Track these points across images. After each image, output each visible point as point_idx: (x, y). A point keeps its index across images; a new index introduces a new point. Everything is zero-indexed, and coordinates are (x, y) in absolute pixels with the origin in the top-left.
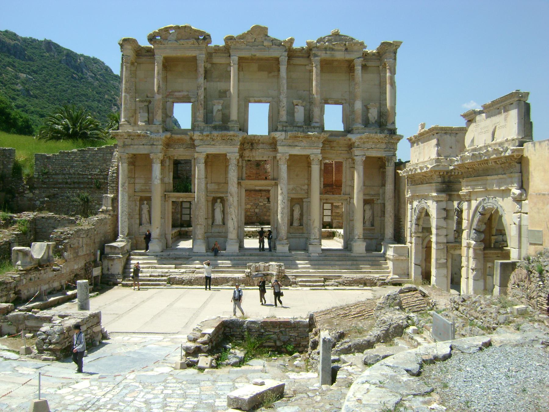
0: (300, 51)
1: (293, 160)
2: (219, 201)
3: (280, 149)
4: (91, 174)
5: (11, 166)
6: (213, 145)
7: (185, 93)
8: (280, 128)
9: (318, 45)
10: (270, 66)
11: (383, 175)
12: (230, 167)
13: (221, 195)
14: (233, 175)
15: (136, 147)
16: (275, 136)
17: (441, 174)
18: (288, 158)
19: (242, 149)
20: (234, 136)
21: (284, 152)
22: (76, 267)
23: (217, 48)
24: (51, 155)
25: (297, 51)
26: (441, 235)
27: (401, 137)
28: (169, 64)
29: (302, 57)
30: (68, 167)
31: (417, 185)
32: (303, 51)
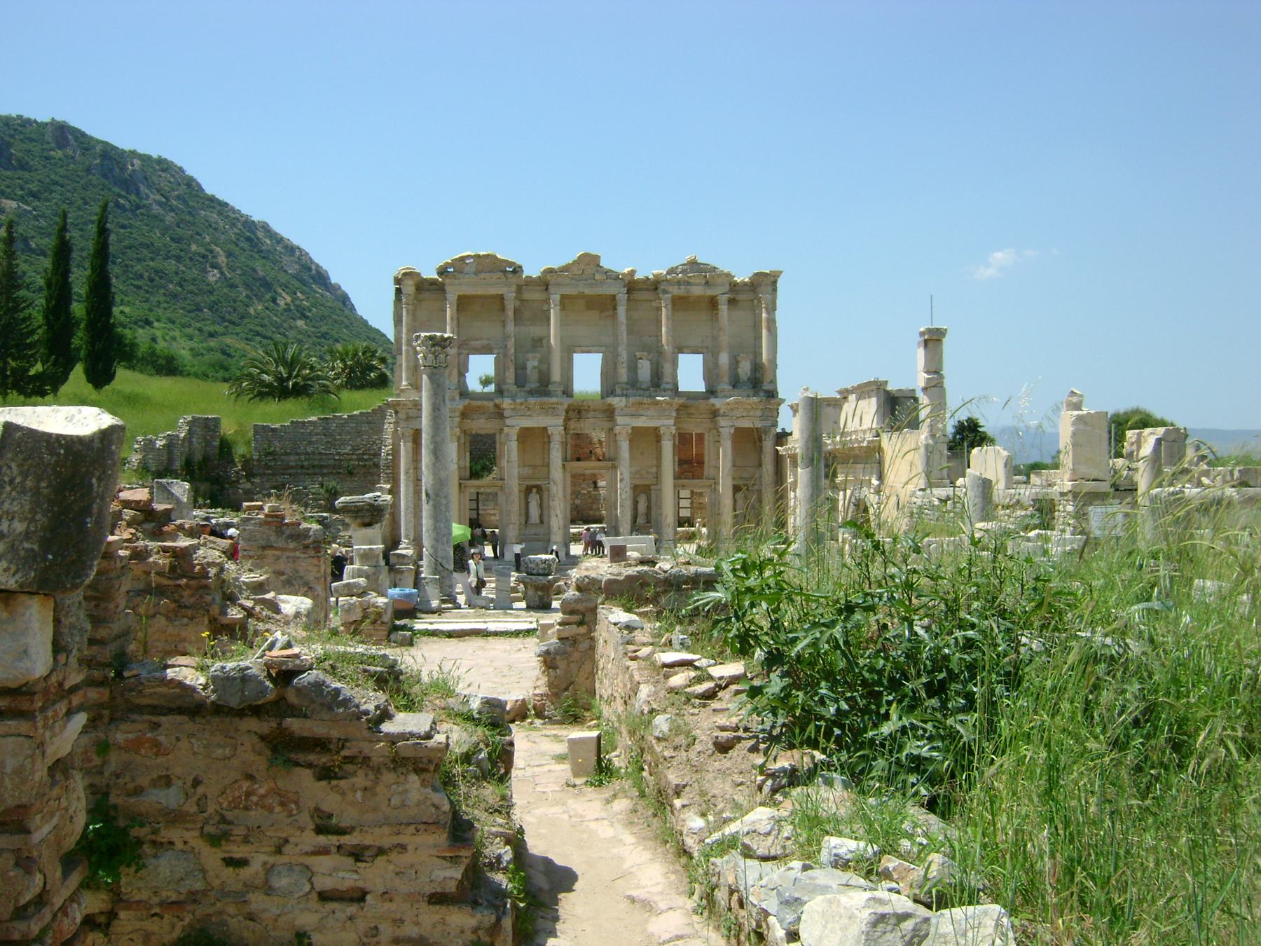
1: (637, 435)
3: (619, 420)
4: (338, 454)
5: (216, 443)
7: (486, 342)
8: (618, 391)
10: (606, 305)
11: (760, 450)
13: (538, 483)
14: (556, 455)
19: (567, 419)
21: (624, 423)
24: (277, 426)
27: (783, 401)
28: (464, 303)
29: (647, 290)
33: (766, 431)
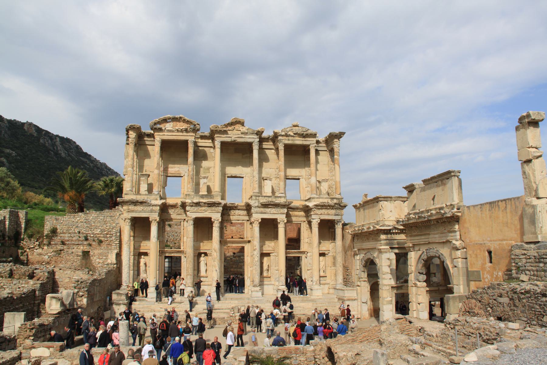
2: (203, 255)
9: (283, 133)
12: (214, 228)
13: (205, 251)
18: (260, 221)
20: (218, 204)
22: (92, 311)
23: (203, 134)
25: (264, 138)
33: (339, 221)
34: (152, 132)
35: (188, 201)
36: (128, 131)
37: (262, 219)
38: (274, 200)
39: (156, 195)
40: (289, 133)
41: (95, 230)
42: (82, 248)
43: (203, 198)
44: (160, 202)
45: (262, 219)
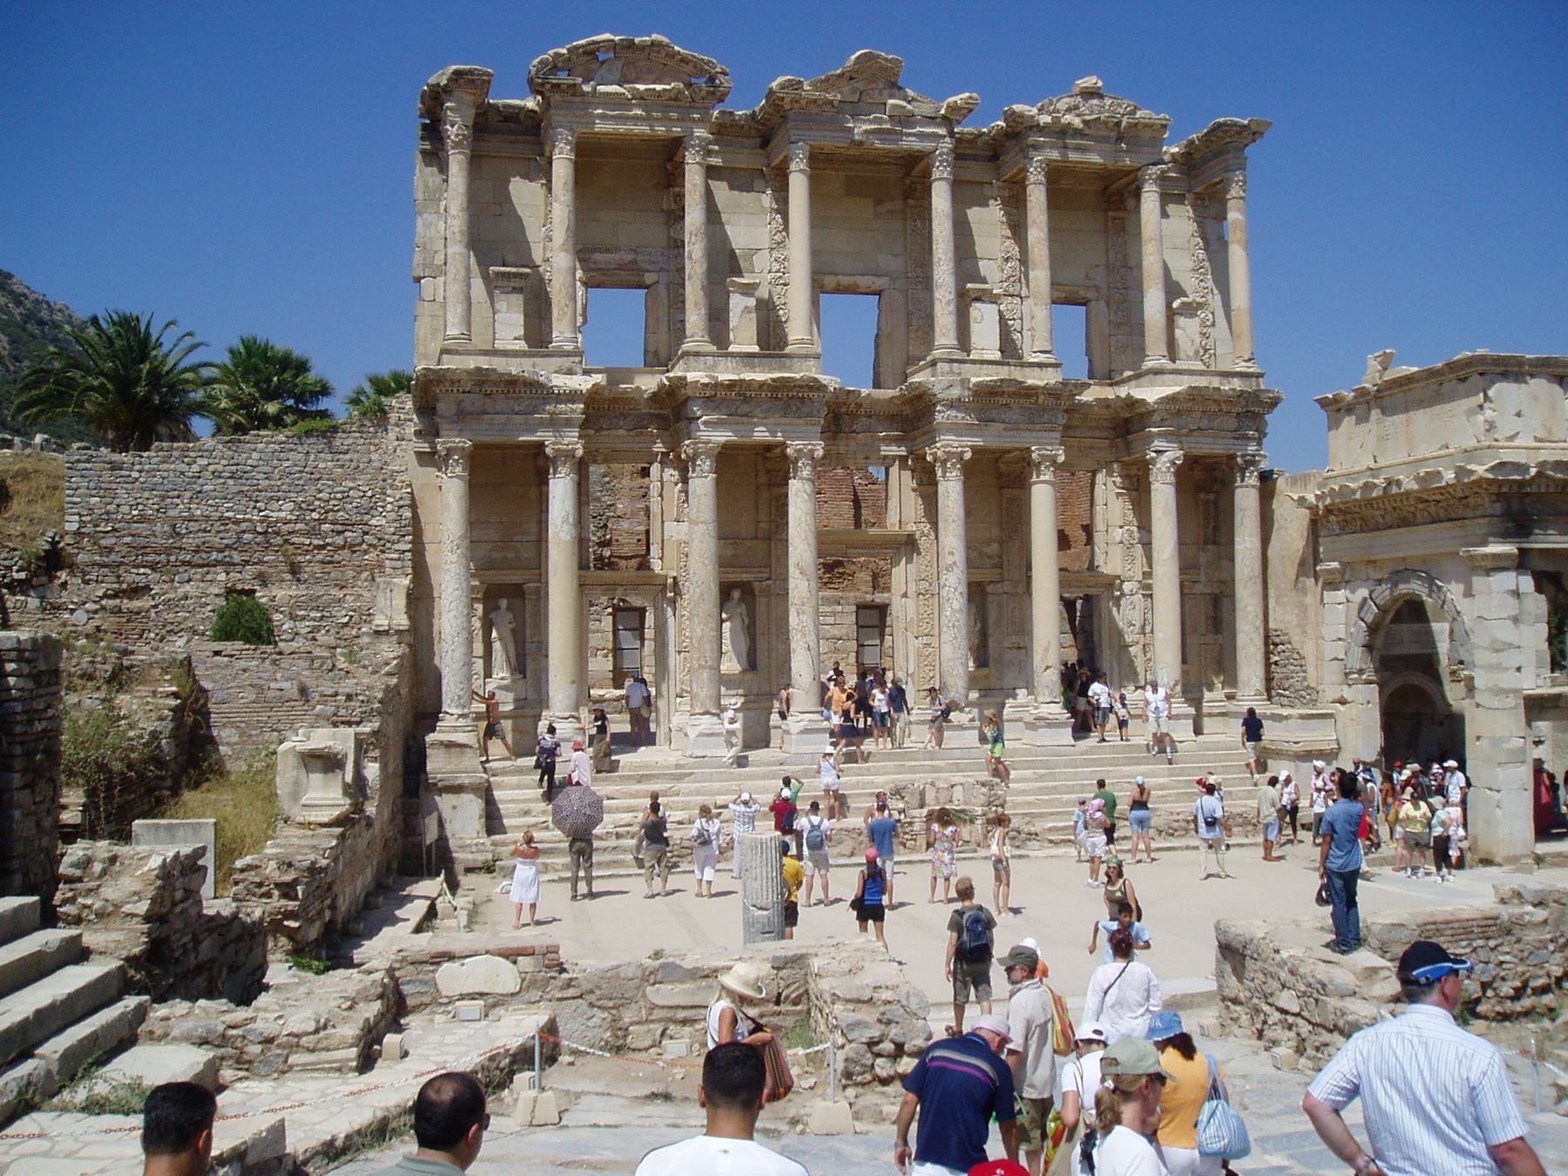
0: (970, 142)
2: (736, 594)
6: (746, 415)
9: (1045, 119)
13: (745, 577)
15: (502, 418)
16: (936, 390)
17: (1504, 490)
18: (968, 456)
20: (811, 388)
23: (728, 119)
26: (1507, 669)
29: (975, 158)
30: (188, 494)
31: (1377, 528)
32: (980, 141)
34: (531, 103)
35: (696, 375)
36: (434, 100)
37: (975, 450)
38: (1017, 374)
39: (568, 354)
40: (1068, 118)
41: (275, 505)
42: (222, 577)
43: (753, 368)
44: (583, 383)
45: (975, 450)
